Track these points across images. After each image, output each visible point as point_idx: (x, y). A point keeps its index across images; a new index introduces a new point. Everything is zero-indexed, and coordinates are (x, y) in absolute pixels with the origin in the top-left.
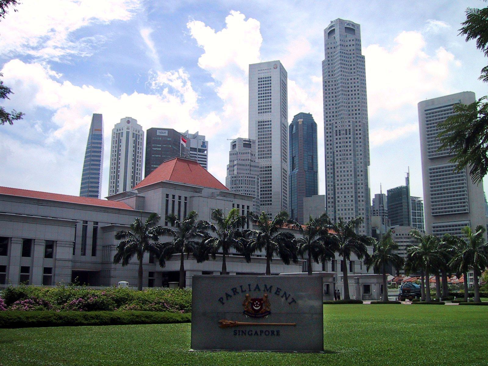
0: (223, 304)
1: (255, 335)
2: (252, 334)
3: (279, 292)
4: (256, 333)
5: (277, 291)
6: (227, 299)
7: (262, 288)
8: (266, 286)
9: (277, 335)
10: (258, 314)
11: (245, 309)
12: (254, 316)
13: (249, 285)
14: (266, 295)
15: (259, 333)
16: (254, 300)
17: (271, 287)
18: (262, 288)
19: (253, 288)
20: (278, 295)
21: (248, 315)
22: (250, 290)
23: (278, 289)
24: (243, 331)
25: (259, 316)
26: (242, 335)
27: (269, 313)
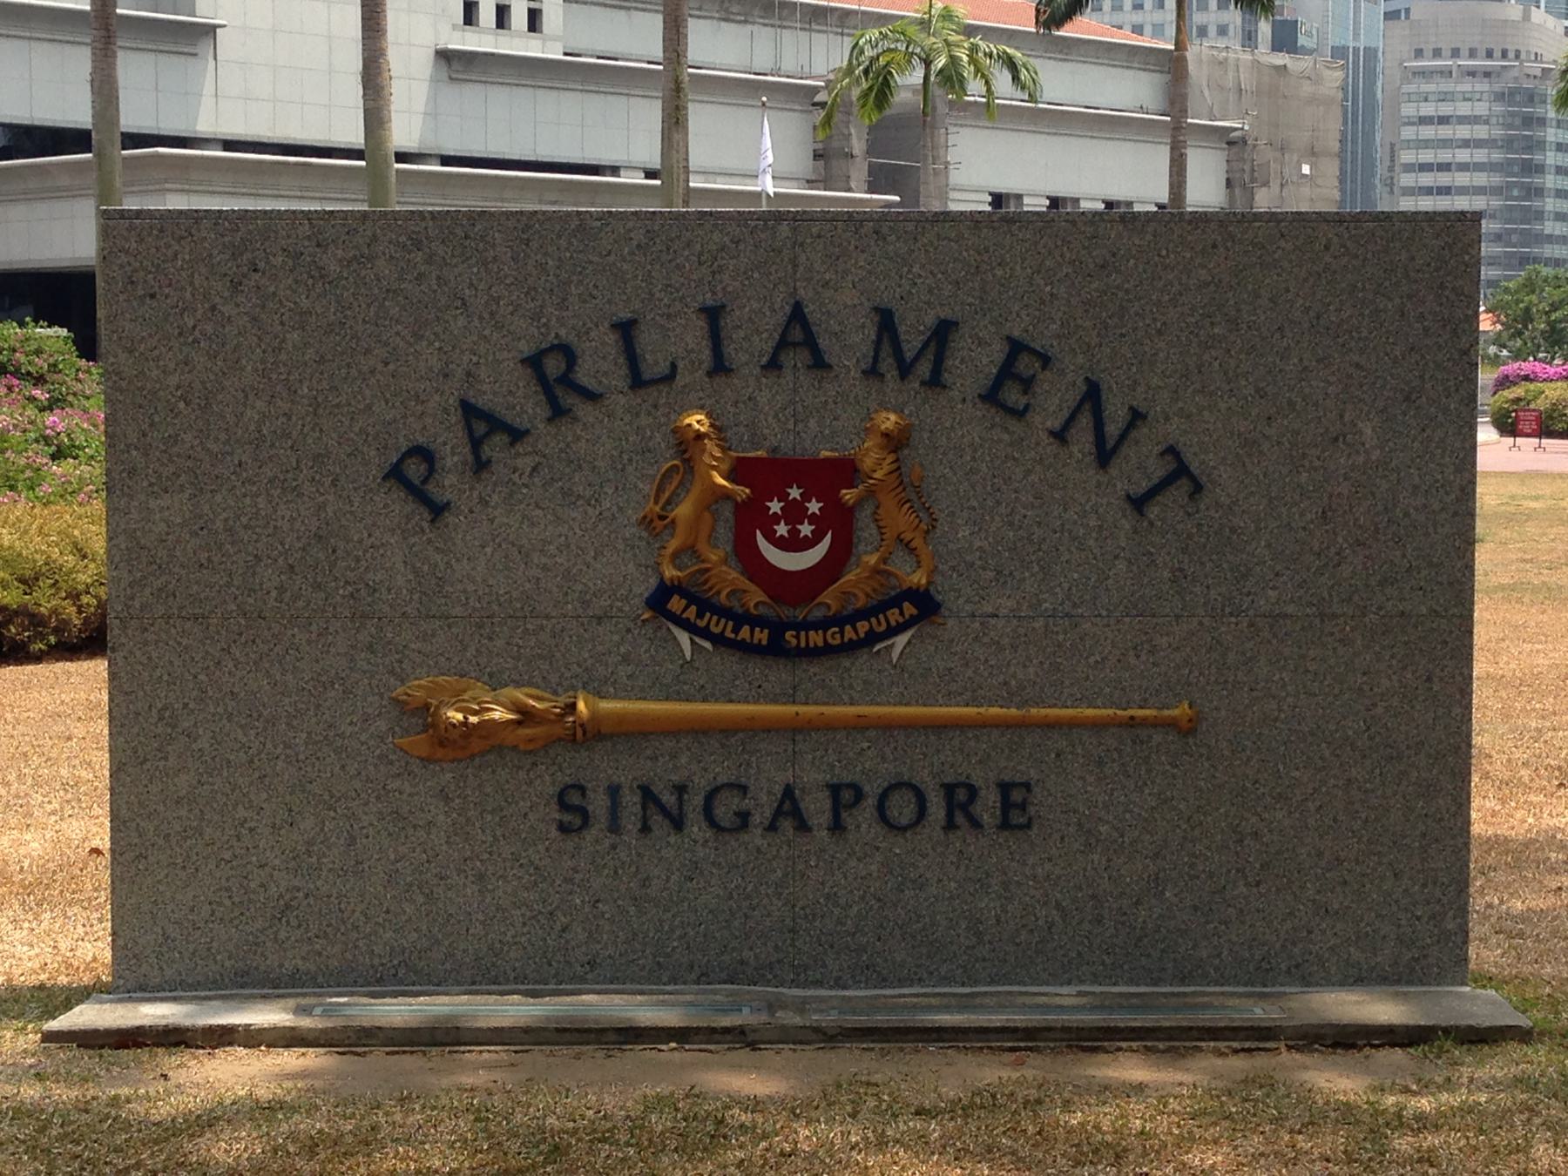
0: (438, 510)
1: (772, 827)
2: (744, 818)
3: (1027, 384)
4: (789, 807)
5: (1007, 372)
6: (481, 466)
7: (849, 340)
8: (886, 322)
9: (1005, 825)
10: (807, 626)
11: (670, 572)
12: (762, 636)
13: (713, 315)
14: (889, 421)
15: (817, 807)
16: (762, 475)
17: (943, 332)
18: (849, 340)
19: (752, 336)
20: (1019, 414)
21: (705, 633)
22: (720, 367)
23: (1016, 347)
24: (647, 794)
25: (816, 638)
26: (645, 829)
27: (926, 605)
